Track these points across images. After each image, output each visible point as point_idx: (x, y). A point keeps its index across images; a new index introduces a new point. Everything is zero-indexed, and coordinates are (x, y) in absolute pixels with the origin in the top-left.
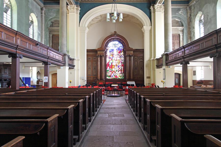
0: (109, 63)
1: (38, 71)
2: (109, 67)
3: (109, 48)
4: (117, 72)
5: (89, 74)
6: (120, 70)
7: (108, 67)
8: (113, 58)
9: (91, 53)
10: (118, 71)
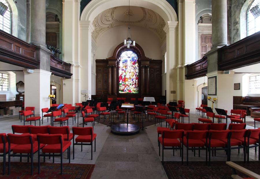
2: (122, 80)
3: (121, 58)
7: (121, 80)
8: (127, 70)
9: (101, 64)
10: (131, 85)
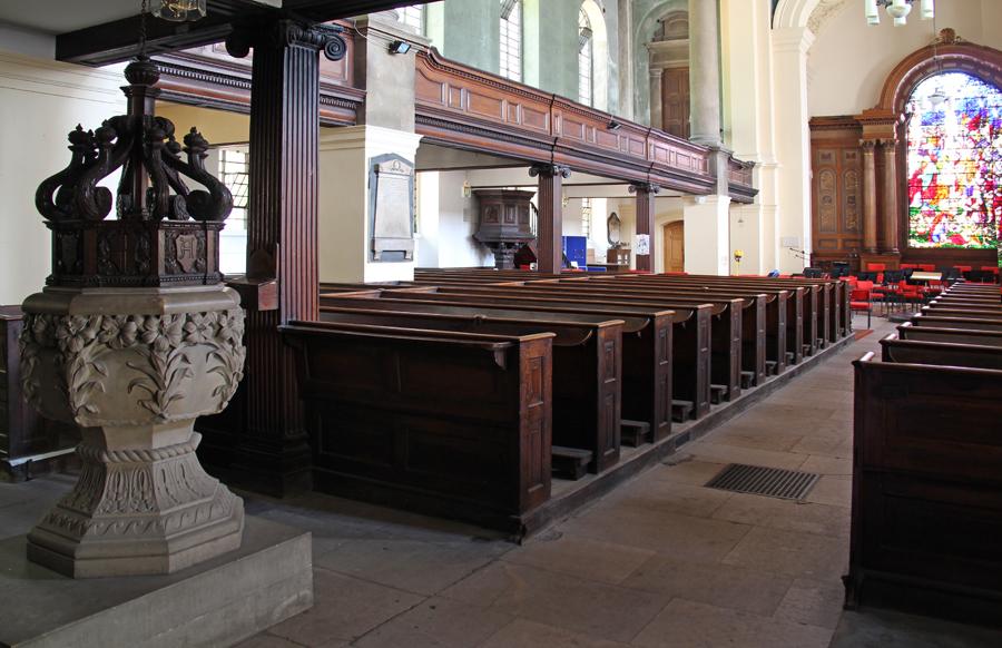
0: (919, 177)
1: (613, 214)
2: (923, 193)
3: (917, 107)
4: (962, 219)
5: (825, 223)
6: (976, 206)
7: (918, 196)
8: (941, 153)
9: (833, 134)
10: (965, 213)
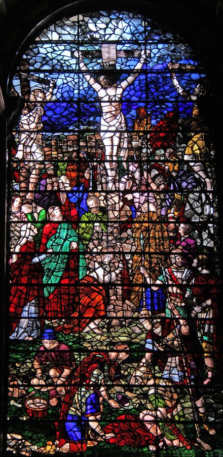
2: (42, 303)
7: (30, 309)
